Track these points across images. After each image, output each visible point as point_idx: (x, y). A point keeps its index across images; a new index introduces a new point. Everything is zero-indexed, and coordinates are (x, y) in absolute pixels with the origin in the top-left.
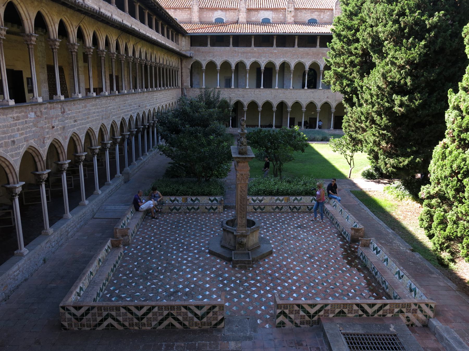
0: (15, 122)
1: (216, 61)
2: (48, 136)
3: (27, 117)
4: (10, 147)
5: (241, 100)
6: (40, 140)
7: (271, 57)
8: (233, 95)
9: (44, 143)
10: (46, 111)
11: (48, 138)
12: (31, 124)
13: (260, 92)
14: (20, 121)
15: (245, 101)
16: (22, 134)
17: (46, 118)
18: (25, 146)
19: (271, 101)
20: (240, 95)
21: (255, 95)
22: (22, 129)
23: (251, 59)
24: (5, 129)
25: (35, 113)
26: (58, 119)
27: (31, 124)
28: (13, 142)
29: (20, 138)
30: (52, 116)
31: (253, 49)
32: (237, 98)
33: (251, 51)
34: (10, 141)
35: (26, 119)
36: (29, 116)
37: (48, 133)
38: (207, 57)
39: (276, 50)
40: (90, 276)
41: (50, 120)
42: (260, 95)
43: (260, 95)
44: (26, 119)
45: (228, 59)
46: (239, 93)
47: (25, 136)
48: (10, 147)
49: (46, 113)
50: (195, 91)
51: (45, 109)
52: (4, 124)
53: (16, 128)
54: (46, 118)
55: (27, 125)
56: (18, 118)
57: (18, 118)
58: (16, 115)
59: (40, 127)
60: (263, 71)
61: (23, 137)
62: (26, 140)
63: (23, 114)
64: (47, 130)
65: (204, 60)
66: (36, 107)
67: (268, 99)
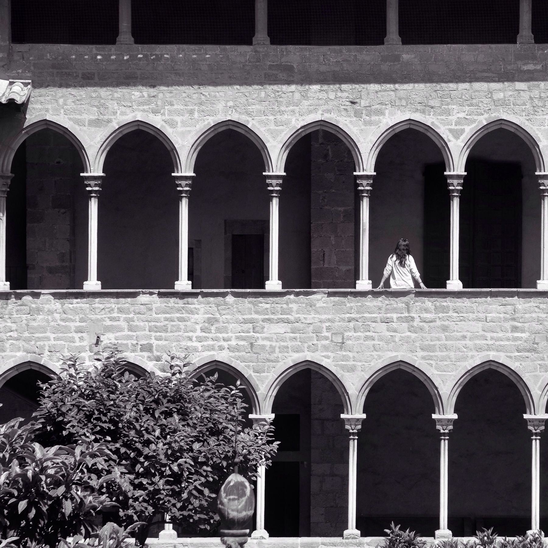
1: (169, 132)
5: (325, 363)
7: (504, 103)
8: (281, 328)
13: (445, 310)
15: (352, 369)
19: (514, 365)
20: (317, 331)
21: (411, 329)
23: (380, 113)
31: (397, 58)
32: (297, 350)
33: (385, 67)
38: (113, 105)
39: (534, 58)
42: (445, 329)
43: (445, 329)
45: (242, 119)
46: (311, 317)
50: (39, 311)
60: (456, 186)
65: (96, 123)
67: (492, 355)
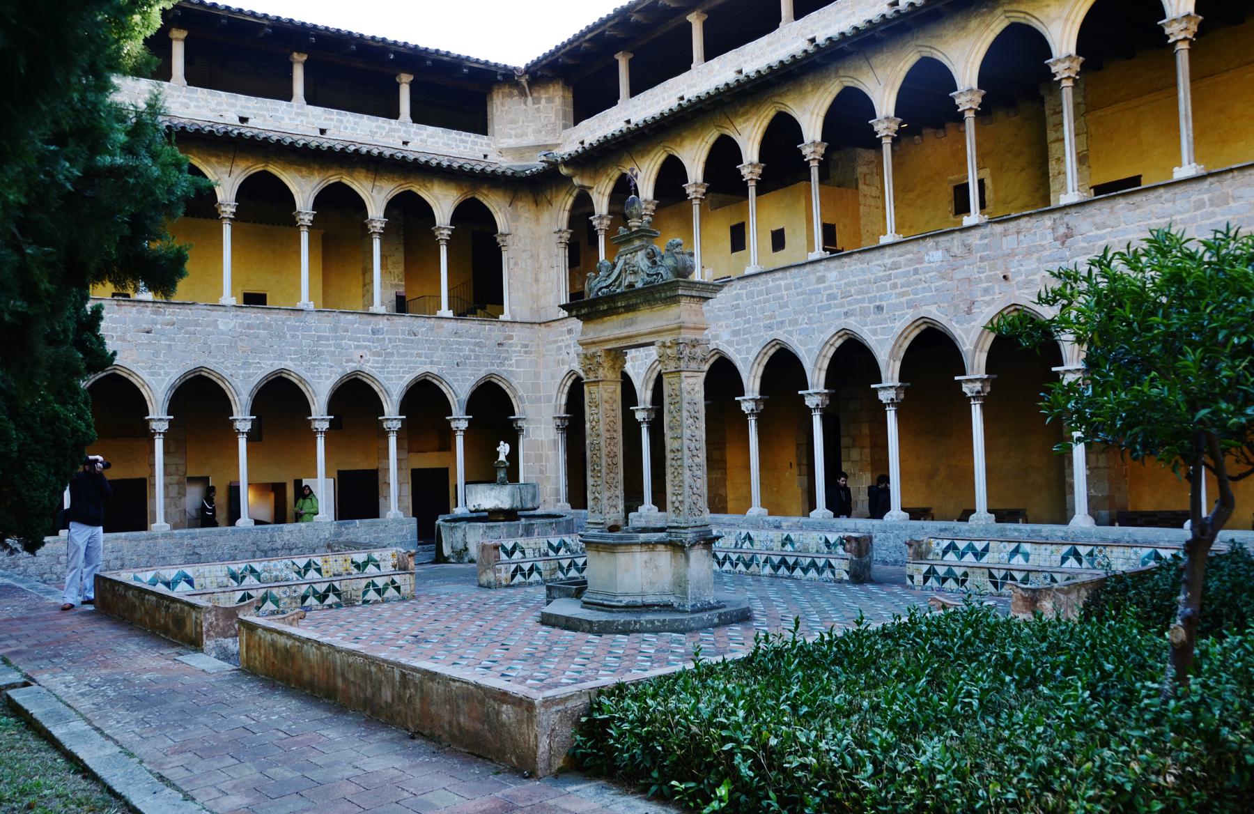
0: (888, 273)
2: (987, 298)
3: (921, 261)
4: (872, 316)
6: (956, 307)
9: (969, 312)
10: (986, 241)
11: (988, 304)
12: (932, 274)
14: (899, 270)
16: (902, 295)
17: (982, 259)
18: (908, 316)
22: (902, 286)
24: (865, 286)
25: (948, 250)
26: (1035, 256)
27: (932, 274)
28: (879, 308)
29: (898, 301)
30: (1009, 251)
34: (872, 306)
35: (918, 266)
36: (926, 258)
37: (986, 291)
40: (744, 538)
41: (1000, 262)
44: (918, 266)
47: (912, 296)
48: (872, 316)
49: (986, 247)
51: (982, 238)
52: (861, 278)
53: (888, 284)
54: (982, 259)
55: (917, 277)
56: (895, 266)
57: (895, 266)
58: (892, 260)
59: (959, 280)
61: (904, 299)
62: (911, 305)
63: (911, 256)
64: (984, 285)
66: (948, 238)
